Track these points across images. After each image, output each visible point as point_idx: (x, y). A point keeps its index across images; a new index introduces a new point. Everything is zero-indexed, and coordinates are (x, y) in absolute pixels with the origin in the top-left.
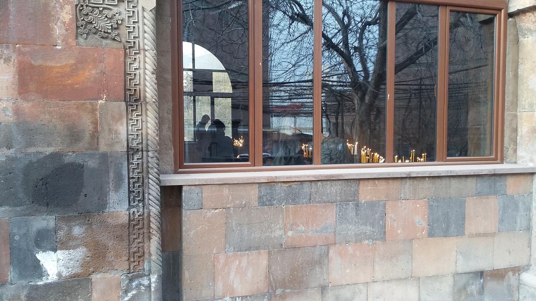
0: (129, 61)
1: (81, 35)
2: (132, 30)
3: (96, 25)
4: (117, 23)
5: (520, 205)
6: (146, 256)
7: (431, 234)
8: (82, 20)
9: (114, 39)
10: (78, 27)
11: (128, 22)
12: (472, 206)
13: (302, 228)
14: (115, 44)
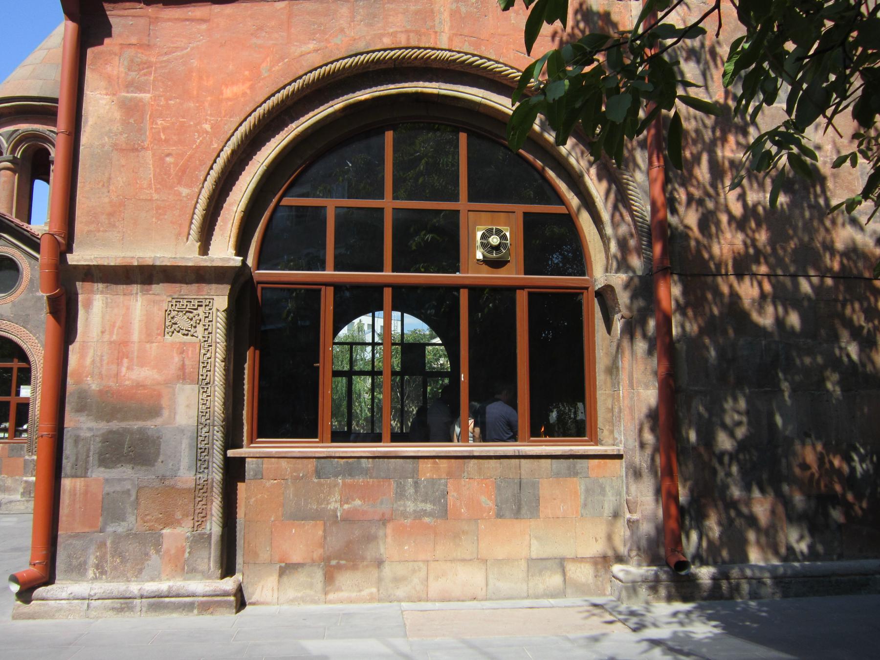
0: (203, 351)
5: (607, 489)
6: (208, 517)
7: (499, 515)
9: (193, 336)
12: (546, 488)
13: (358, 502)
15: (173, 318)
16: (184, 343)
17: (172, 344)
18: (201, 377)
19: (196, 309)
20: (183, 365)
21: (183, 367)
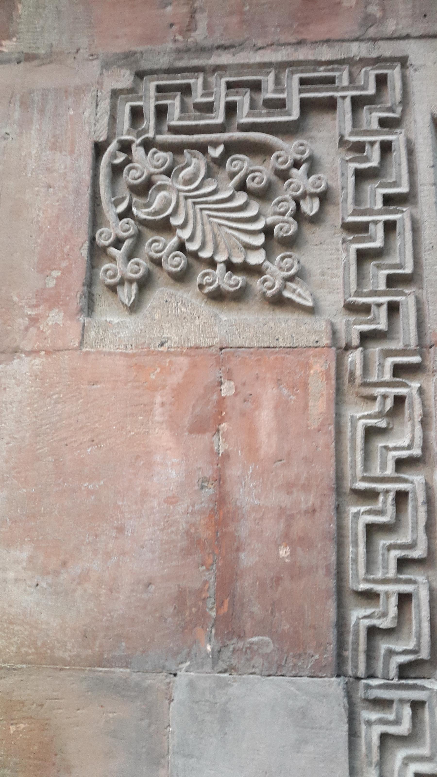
1: (113, 289)
2: (378, 244)
3: (185, 234)
4: (298, 214)
8: (121, 216)
9: (279, 302)
10: (96, 253)
11: (357, 200)
14: (284, 327)
15: (144, 189)
17: (143, 358)
20: (221, 512)
21: (217, 528)
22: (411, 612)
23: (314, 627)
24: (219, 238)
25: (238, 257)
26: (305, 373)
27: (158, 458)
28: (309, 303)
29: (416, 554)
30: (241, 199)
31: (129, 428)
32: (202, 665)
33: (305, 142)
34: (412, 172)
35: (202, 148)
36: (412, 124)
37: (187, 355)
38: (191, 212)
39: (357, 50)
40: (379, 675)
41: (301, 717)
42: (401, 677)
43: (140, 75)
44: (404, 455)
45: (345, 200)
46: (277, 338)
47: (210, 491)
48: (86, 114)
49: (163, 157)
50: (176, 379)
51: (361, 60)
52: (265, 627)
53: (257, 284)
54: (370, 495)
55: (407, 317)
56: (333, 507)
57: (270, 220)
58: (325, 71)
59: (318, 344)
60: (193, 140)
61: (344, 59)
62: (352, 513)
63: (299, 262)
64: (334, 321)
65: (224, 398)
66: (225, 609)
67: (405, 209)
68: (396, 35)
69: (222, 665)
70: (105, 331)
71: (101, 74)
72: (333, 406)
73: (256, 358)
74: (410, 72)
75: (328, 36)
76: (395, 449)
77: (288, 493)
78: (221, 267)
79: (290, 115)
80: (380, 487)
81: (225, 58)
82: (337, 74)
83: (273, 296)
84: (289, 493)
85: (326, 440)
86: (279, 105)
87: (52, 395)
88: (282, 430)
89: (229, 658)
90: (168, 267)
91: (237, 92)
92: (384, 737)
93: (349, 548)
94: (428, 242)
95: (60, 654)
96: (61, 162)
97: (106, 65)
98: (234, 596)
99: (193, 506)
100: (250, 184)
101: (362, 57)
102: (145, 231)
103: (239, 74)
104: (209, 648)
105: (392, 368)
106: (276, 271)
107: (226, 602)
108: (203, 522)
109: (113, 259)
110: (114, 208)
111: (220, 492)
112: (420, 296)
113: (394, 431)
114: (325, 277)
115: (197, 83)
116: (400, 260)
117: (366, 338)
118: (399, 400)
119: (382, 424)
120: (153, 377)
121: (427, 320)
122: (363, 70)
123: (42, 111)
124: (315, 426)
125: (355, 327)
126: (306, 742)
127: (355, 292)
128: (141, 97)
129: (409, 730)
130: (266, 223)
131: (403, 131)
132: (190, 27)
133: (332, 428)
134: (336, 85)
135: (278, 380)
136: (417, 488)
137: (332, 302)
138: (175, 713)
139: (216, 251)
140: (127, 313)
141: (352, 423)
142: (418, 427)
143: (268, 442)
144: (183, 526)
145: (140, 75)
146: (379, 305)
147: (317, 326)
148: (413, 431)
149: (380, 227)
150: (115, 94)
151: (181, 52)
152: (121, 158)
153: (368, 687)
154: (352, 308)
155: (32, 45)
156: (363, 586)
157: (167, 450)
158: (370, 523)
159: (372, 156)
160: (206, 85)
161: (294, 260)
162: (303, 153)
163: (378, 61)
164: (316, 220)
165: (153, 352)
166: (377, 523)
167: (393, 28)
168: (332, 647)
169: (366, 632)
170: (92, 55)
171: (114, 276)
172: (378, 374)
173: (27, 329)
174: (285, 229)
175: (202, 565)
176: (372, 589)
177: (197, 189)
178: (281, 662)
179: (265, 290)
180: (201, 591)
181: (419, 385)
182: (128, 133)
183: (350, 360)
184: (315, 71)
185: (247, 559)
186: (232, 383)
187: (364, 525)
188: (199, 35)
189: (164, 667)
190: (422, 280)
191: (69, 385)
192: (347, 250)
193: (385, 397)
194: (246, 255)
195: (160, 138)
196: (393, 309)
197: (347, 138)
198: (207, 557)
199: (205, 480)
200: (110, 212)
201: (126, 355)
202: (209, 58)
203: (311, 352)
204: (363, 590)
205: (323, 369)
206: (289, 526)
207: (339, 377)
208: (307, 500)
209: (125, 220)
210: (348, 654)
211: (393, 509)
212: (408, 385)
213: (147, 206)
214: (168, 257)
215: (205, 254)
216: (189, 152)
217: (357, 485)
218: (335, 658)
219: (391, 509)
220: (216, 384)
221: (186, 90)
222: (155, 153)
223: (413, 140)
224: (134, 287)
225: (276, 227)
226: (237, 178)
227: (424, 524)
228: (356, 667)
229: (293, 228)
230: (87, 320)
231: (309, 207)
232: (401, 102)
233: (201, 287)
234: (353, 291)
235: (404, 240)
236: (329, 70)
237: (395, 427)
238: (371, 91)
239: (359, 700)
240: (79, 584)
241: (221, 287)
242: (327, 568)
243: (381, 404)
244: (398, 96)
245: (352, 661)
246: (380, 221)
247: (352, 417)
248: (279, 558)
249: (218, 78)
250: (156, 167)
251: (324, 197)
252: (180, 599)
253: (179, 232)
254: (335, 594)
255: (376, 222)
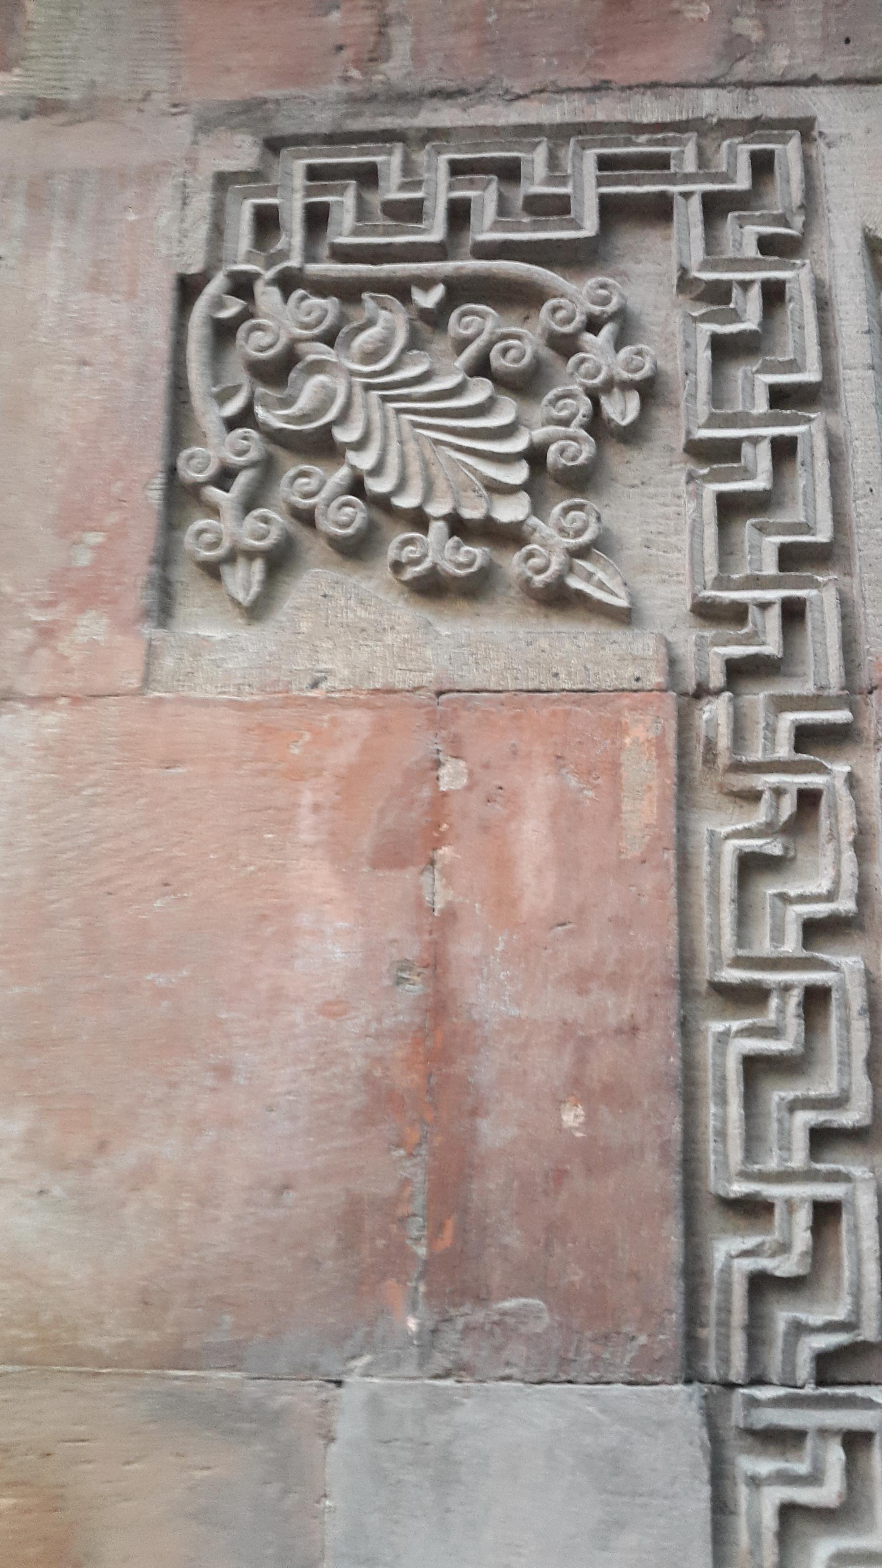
1: (212, 570)
2: (760, 483)
3: (365, 461)
4: (597, 424)
8: (231, 424)
9: (558, 599)
11: (717, 397)
14: (570, 649)
15: (277, 371)
16: (444, 699)
17: (276, 712)
18: (731, 1252)
19: (575, 258)
20: (440, 1033)
21: (430, 1071)
22: (838, 1243)
23: (635, 1276)
24: (434, 470)
25: (475, 508)
26: (613, 743)
27: (305, 920)
28: (622, 602)
29: (850, 1117)
30: (480, 391)
31: (243, 858)
32: (398, 1361)
33: (610, 281)
34: (827, 343)
35: (400, 290)
36: (825, 251)
37: (367, 705)
38: (376, 417)
39: (712, 104)
40: (775, 1380)
41: (610, 1472)
42: (820, 1382)
43: (274, 146)
44: (820, 912)
45: (693, 396)
46: (555, 671)
47: (415, 988)
48: (163, 220)
49: (320, 306)
50: (344, 756)
51: (721, 123)
52: (531, 1278)
53: (513, 564)
54: (751, 997)
55: (822, 630)
56: (674, 1020)
57: (539, 434)
58: (650, 143)
59: (639, 685)
60: (382, 274)
61: (687, 121)
62: (714, 1033)
63: (599, 519)
64: (670, 638)
65: (445, 794)
66: (447, 1238)
67: (813, 416)
68: (790, 77)
69: (441, 1361)
70: (196, 655)
71: (195, 142)
72: (672, 810)
73: (512, 713)
74: (820, 149)
75: (654, 77)
76: (803, 899)
77: (580, 993)
78: (438, 528)
79: (579, 228)
80: (771, 978)
81: (446, 116)
82: (674, 150)
83: (547, 586)
84: (582, 991)
85: (657, 880)
86: (557, 207)
87: (81, 789)
88: (566, 860)
89: (455, 1345)
90: (327, 525)
91: (472, 182)
92: (788, 1512)
93: (708, 1107)
94: (861, 480)
95: (90, 1341)
96: (109, 313)
97: (205, 125)
98: (465, 1211)
99: (379, 1020)
100: (497, 361)
101: (722, 117)
102: (281, 454)
103: (477, 147)
104: (412, 1324)
105: (793, 732)
106: (552, 536)
107: (450, 1224)
108: (400, 1054)
109: (214, 511)
110: (216, 408)
111: (437, 992)
112: (846, 589)
113: (799, 863)
114: (653, 551)
115: (390, 163)
116: (806, 517)
117: (739, 672)
118: (809, 800)
119: (774, 847)
120: (296, 751)
121: (862, 638)
122: (725, 144)
123: (71, 215)
124: (634, 852)
125: (716, 649)
126: (620, 1525)
127: (715, 579)
128: (275, 188)
129: (840, 1496)
130: (531, 440)
131: (807, 261)
132: (377, 54)
133: (670, 856)
134: (672, 170)
135: (558, 757)
136: (847, 981)
137: (668, 599)
138: (338, 1466)
139: (428, 493)
140: (240, 621)
141: (711, 847)
142: (849, 854)
143: (536, 884)
144: (358, 1063)
145: (274, 146)
146: (764, 606)
147: (638, 648)
148: (837, 862)
149: (765, 448)
150: (223, 181)
151: (358, 101)
152: (233, 308)
153: (753, 1403)
154: (707, 612)
155: (53, 83)
156: (739, 1188)
157: (326, 903)
158: (752, 1053)
159: (745, 311)
160: (408, 168)
161: (588, 514)
162: (606, 301)
163: (755, 126)
164: (632, 435)
165: (296, 698)
166: (766, 1052)
167: (785, 62)
168: (675, 1319)
169: (746, 1286)
170: (175, 106)
171: (214, 545)
172: (765, 746)
173: (30, 651)
174: (570, 452)
175: (398, 1146)
176: (757, 1194)
177: (389, 370)
178: (567, 1351)
179: (529, 574)
180: (395, 1201)
181: (848, 769)
182: (248, 261)
183: (705, 716)
184: (629, 143)
185: (494, 1133)
186: (462, 764)
187: (740, 1057)
188: (396, 70)
189: (314, 1367)
190: (849, 557)
191: (116, 768)
192: (698, 496)
193: (778, 792)
194: (490, 502)
195: (314, 269)
196: (793, 613)
197: (695, 274)
198: (408, 1130)
199: (405, 965)
200: (209, 415)
201: (240, 706)
202: (415, 115)
203: (626, 700)
204: (738, 1195)
205: (651, 735)
206: (581, 1061)
207: (683, 753)
208: (618, 1007)
209: (240, 431)
210: (709, 1333)
211: (799, 1025)
212: (826, 768)
213: (287, 403)
214: (328, 506)
215: (406, 501)
216: (372, 298)
217: (723, 974)
218: (680, 1342)
219: (794, 1026)
220: (428, 765)
221: (368, 176)
222: (303, 298)
223: (827, 282)
224: (258, 566)
225: (553, 448)
226: (471, 351)
227: (864, 1055)
228: (725, 1360)
229: (586, 451)
230: (160, 633)
231: (619, 408)
232: (801, 206)
233: (397, 567)
234: (710, 577)
235: (812, 477)
236: (657, 143)
237: (800, 856)
238: (743, 182)
239: (732, 1433)
240: (134, 1189)
241: (439, 567)
242: (664, 1148)
243: (771, 806)
244: (797, 195)
245: (718, 1349)
246: (764, 438)
247: (712, 833)
248: (560, 1131)
249: (433, 153)
250: (306, 326)
251: (649, 390)
252: (352, 1218)
253: (351, 456)
254: (681, 1204)
255: (755, 441)
